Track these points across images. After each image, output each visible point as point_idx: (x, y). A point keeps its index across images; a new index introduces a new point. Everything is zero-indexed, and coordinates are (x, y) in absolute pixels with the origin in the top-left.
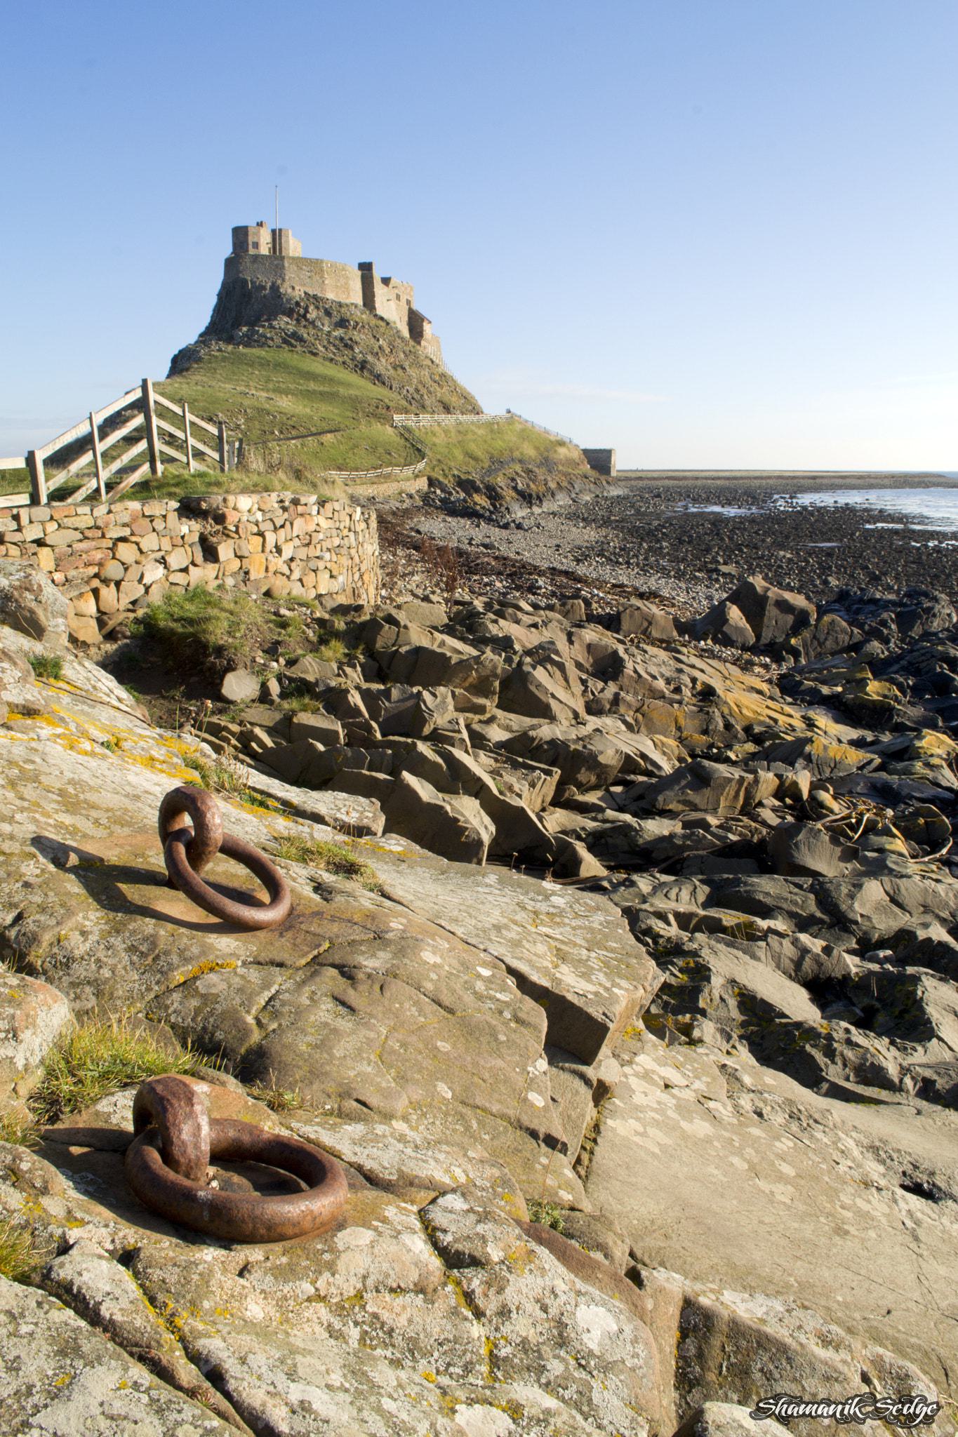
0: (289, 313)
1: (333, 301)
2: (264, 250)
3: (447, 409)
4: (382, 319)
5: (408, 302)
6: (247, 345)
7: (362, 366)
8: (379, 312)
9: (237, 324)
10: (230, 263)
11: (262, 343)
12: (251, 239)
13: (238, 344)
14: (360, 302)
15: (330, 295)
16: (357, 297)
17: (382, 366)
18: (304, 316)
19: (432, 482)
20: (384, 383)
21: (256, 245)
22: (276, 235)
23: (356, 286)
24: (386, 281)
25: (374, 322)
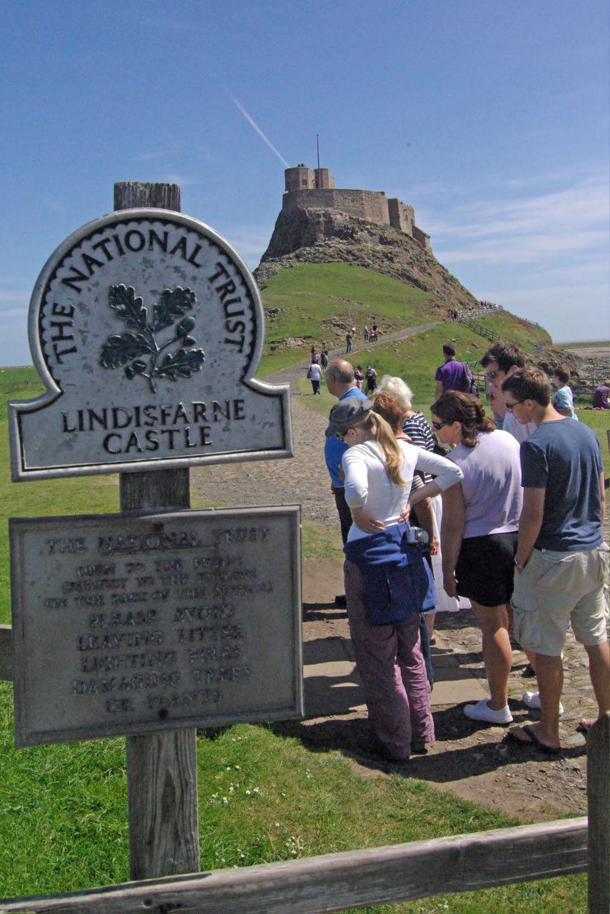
4: (407, 235)
5: (412, 221)
9: (297, 245)
12: (301, 178)
14: (388, 223)
15: (369, 219)
17: (415, 273)
20: (419, 287)
21: (305, 182)
22: (319, 173)
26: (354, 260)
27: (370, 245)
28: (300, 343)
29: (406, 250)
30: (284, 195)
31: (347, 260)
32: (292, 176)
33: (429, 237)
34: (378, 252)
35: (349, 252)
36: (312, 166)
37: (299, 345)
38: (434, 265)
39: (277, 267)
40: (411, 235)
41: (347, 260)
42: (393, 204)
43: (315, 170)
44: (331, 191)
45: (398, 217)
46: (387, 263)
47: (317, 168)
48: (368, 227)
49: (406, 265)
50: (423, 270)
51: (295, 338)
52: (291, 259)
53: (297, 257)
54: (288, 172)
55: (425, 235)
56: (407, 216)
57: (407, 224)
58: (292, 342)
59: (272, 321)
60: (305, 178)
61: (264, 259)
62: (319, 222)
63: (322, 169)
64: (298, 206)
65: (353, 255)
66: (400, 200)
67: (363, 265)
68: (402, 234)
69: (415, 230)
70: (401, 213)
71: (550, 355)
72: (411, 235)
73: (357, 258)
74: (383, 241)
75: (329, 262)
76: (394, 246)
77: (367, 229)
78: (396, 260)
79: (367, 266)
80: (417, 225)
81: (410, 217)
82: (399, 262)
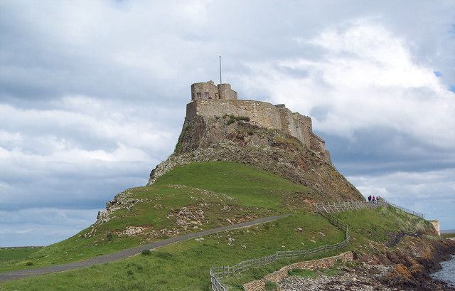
0: (230, 137)
3: (344, 198)
4: (295, 138)
5: (310, 128)
9: (196, 147)
15: (260, 124)
17: (298, 171)
18: (242, 138)
25: (290, 141)
28: (139, 231)
37: (136, 234)
38: (321, 164)
46: (271, 161)
49: (289, 164)
50: (306, 169)
54: (193, 86)
57: (303, 131)
60: (207, 91)
62: (214, 127)
69: (313, 135)
70: (291, 120)
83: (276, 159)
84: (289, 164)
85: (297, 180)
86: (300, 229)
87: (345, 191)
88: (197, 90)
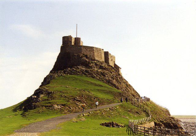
1: (97, 61)
2: (73, 44)
4: (111, 66)
5: (114, 62)
6: (71, 74)
7: (109, 82)
8: (110, 64)
9: (66, 67)
10: (62, 48)
11: (76, 73)
13: (68, 74)
14: (104, 61)
16: (103, 59)
17: (114, 81)
19: (156, 124)
21: (71, 42)
23: (103, 56)
24: (110, 54)
26: (88, 74)
27: (96, 69)
28: (60, 107)
29: (111, 72)
30: (61, 47)
31: (86, 74)
32: (66, 40)
33: (121, 68)
34: (99, 72)
35: (86, 71)
36: (74, 36)
39: (56, 75)
40: (113, 67)
41: (86, 74)
42: (106, 54)
43: (75, 38)
44: (81, 46)
45: (109, 59)
47: (76, 37)
48: (96, 62)
50: (117, 80)
51: (58, 105)
52: (62, 72)
53: (64, 72)
55: (119, 67)
56: (112, 59)
58: (56, 106)
59: (49, 97)
61: (51, 72)
63: (78, 38)
64: (67, 51)
65: (88, 73)
66: (110, 52)
67: (92, 77)
68: (110, 66)
69: (115, 65)
70: (109, 57)
71: (170, 120)
72: (113, 67)
73: (90, 74)
74: (101, 67)
75: (78, 75)
76: (106, 70)
77: (95, 63)
78: (106, 76)
79: (94, 77)
80: (116, 63)
81: (113, 60)
82: (107, 77)
83: (104, 76)
84: (110, 79)
85: (114, 85)
86: (129, 110)
87: (133, 92)
88: (66, 39)
